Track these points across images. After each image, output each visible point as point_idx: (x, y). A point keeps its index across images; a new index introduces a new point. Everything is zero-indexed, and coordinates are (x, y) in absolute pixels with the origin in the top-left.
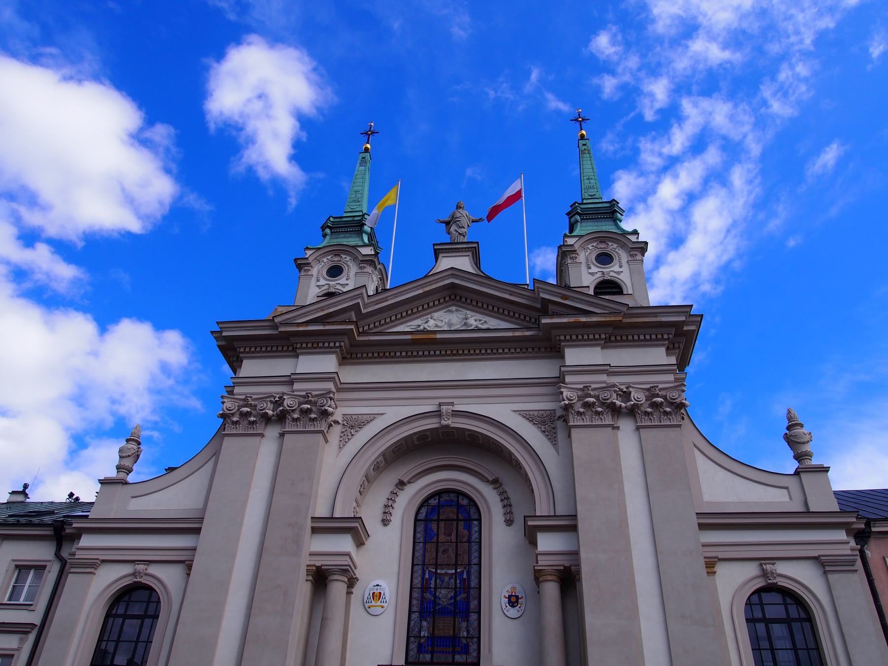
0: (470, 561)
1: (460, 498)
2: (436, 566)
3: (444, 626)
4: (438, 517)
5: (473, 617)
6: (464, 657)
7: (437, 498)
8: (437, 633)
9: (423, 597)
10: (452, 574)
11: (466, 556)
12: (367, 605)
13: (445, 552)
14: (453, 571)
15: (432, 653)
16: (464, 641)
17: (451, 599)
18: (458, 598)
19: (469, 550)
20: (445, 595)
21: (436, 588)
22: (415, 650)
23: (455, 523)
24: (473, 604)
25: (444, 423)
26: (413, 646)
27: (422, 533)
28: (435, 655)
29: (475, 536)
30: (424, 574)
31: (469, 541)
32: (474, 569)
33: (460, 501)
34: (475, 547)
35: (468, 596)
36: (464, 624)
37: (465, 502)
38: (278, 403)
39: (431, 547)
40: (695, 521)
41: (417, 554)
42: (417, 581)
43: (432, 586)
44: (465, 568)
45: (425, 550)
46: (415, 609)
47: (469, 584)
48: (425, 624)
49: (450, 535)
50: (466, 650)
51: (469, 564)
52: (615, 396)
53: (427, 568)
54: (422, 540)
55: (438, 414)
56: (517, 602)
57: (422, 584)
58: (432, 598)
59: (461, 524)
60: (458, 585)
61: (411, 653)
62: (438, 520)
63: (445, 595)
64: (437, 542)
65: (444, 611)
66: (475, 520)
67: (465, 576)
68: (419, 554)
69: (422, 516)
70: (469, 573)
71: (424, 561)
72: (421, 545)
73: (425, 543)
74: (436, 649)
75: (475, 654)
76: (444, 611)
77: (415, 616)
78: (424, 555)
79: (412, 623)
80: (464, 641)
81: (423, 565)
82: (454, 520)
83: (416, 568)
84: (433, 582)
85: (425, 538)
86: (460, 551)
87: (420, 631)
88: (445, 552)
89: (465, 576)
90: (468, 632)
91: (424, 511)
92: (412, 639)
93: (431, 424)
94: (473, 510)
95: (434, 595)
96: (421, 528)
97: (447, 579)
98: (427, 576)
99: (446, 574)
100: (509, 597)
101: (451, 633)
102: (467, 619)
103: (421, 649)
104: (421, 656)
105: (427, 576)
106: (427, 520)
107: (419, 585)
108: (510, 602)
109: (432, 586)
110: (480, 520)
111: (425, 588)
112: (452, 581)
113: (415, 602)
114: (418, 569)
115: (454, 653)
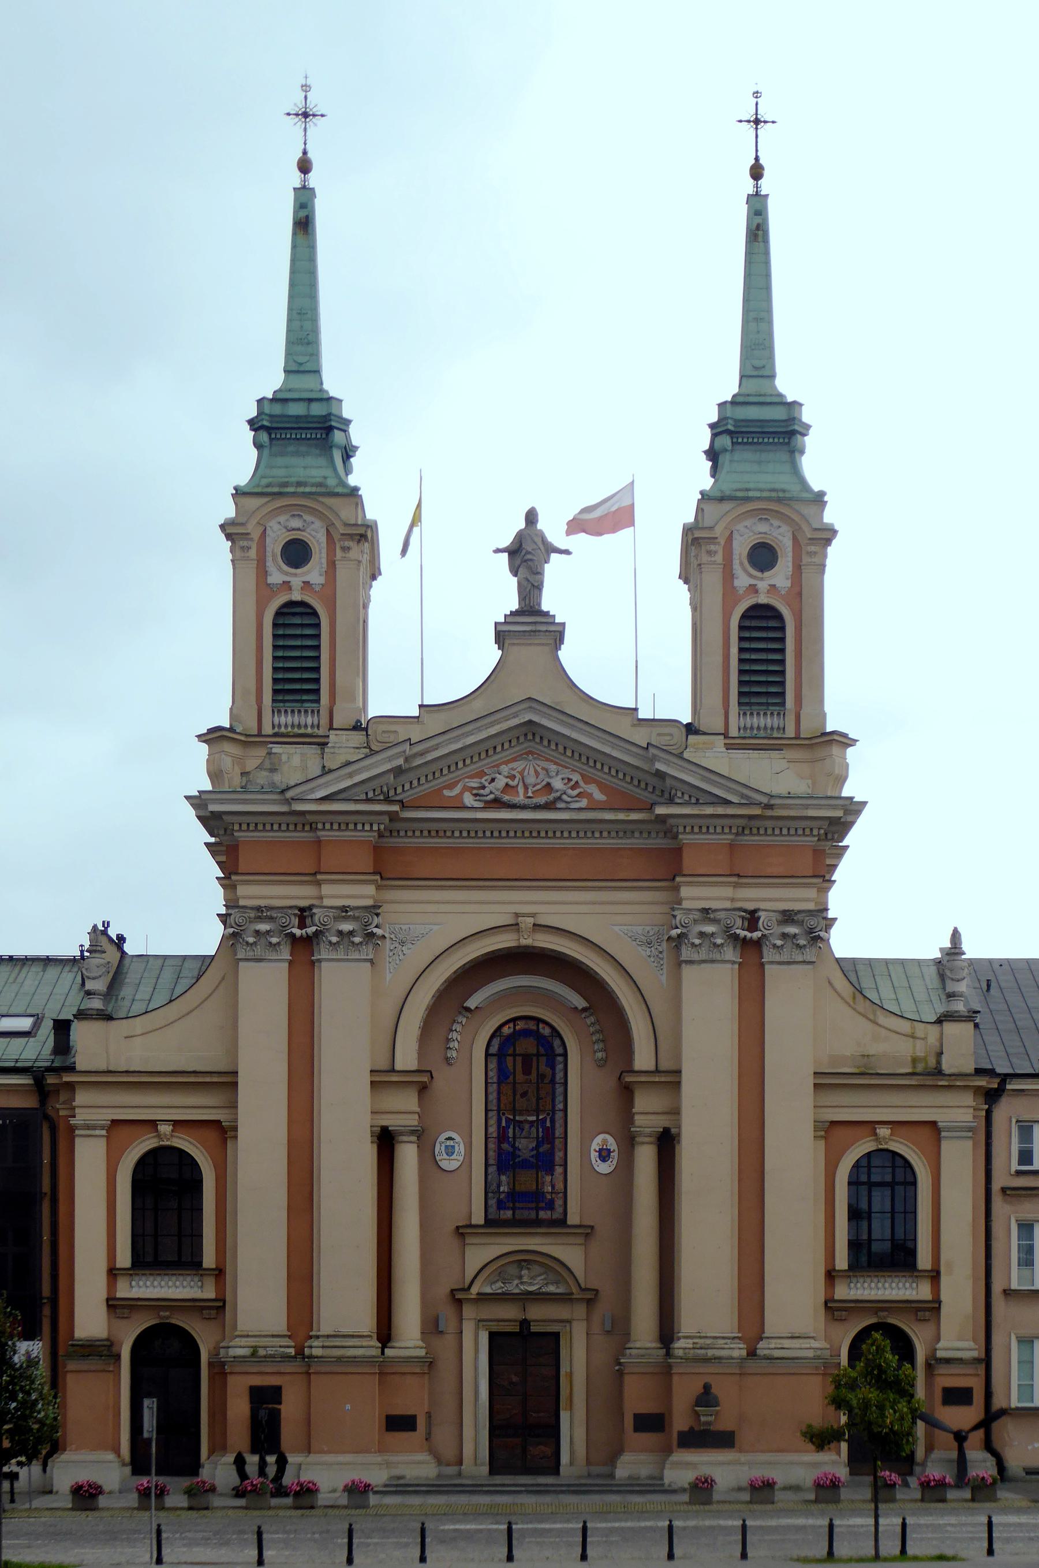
0: (554, 1106)
1: (541, 1026)
2: (514, 1111)
3: (526, 1181)
4: (515, 1050)
5: (559, 1170)
6: (549, 1213)
7: (511, 1025)
8: (517, 1188)
9: (499, 1148)
10: (532, 1122)
11: (549, 1099)
12: (438, 1158)
13: (524, 1094)
14: (534, 1118)
15: (514, 1209)
16: (549, 1197)
17: (532, 1150)
18: (541, 1150)
19: (554, 1093)
20: (525, 1146)
21: (514, 1137)
22: (495, 1206)
23: (534, 1059)
24: (559, 1155)
25: (524, 942)
26: (493, 1202)
27: (495, 1070)
28: (517, 1212)
29: (559, 1076)
30: (499, 1120)
31: (553, 1081)
32: (559, 1115)
33: (541, 1030)
34: (559, 1089)
35: (553, 1148)
36: (548, 1178)
37: (546, 1031)
38: (304, 914)
39: (507, 1089)
40: (811, 1081)
41: (491, 1097)
42: (493, 1130)
43: (511, 1135)
44: (548, 1114)
45: (499, 1093)
46: (491, 1161)
47: (554, 1134)
48: (503, 1178)
49: (530, 1073)
50: (550, 1206)
51: (554, 1111)
52: (739, 922)
53: (504, 1114)
54: (495, 1080)
55: (515, 927)
56: (609, 1156)
57: (499, 1132)
58: (511, 1149)
59: (543, 1060)
60: (541, 1135)
61: (491, 1210)
62: (514, 1055)
63: (525, 1146)
64: (515, 1083)
65: (525, 1164)
66: (560, 1055)
67: (548, 1124)
68: (493, 1097)
69: (494, 1050)
70: (553, 1121)
71: (499, 1106)
72: (495, 1086)
73: (499, 1083)
74: (517, 1205)
75: (560, 1210)
76: (525, 1164)
77: (492, 1169)
78: (499, 1099)
79: (490, 1177)
80: (549, 1197)
81: (499, 1110)
82: (534, 1055)
83: (490, 1114)
84: (511, 1131)
85: (499, 1078)
86: (543, 1094)
87: (499, 1186)
88: (524, 1094)
89: (548, 1124)
90: (553, 1187)
91: (496, 1042)
92: (490, 1195)
93: (505, 941)
94: (557, 1043)
95: (513, 1146)
96: (493, 1065)
97: (527, 1126)
98: (504, 1124)
99: (526, 1121)
100: (600, 1151)
101: (534, 1187)
102: (551, 1171)
103: (501, 1205)
104: (502, 1212)
105: (504, 1124)
106: (501, 1055)
107: (495, 1135)
108: (600, 1156)
109: (511, 1135)
110: (565, 1055)
111: (502, 1137)
112: (534, 1130)
113: (491, 1153)
114: (493, 1114)
115: (538, 1209)
